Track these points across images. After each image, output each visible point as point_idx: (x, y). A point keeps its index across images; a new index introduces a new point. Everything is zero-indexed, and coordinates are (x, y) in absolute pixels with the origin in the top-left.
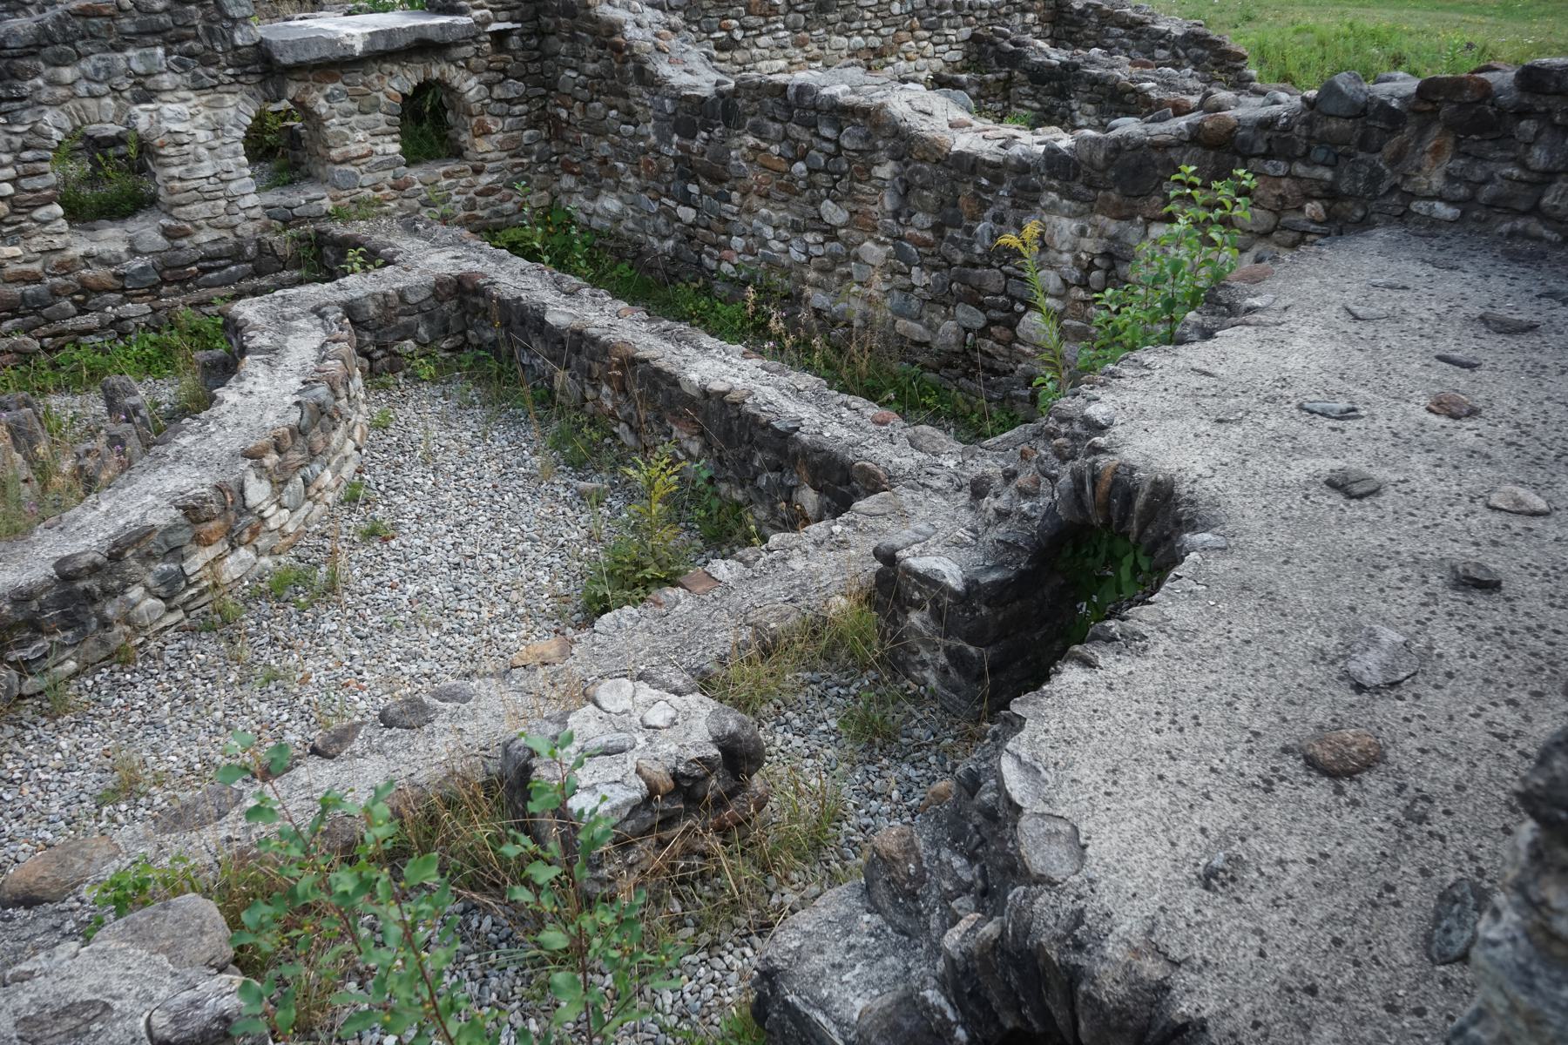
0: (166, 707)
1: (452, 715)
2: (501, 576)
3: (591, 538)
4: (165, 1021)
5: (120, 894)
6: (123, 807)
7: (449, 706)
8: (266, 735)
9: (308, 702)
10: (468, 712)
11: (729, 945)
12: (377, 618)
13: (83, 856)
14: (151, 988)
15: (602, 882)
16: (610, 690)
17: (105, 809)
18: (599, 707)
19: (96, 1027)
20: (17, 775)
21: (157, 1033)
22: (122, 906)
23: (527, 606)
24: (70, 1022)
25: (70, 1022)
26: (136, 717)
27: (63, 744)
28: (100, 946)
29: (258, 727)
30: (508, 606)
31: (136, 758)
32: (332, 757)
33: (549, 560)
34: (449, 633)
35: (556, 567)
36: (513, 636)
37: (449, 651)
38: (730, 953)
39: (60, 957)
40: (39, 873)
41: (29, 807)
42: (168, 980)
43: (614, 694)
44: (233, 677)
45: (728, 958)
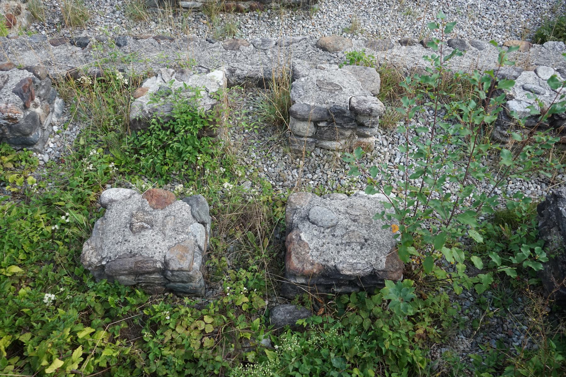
0: (373, 9)
1: (473, 52)
2: (507, 11)
3: (552, 11)
4: (355, 101)
5: (353, 58)
6: (349, 36)
7: (474, 49)
8: (399, 33)
9: (417, 28)
10: (480, 54)
11: (533, 181)
12: (453, 8)
13: (343, 42)
14: (354, 90)
15: (502, 135)
16: (544, 70)
17: (344, 34)
18: (537, 74)
19: (337, 93)
20: (324, 11)
21: (352, 103)
22: (352, 62)
23: (511, 27)
24: (330, 87)
25: (330, 87)
26: (363, 8)
27: (339, 7)
28: (344, 70)
29: (398, 29)
30: (503, 24)
31: (358, 22)
32: (426, 48)
33: (529, 12)
34: (476, 24)
35: (530, 16)
36: (500, 36)
37: (473, 31)
38: (532, 184)
39: (333, 68)
40: (330, 42)
41: (324, 23)
42: (360, 90)
43: (545, 72)
44: (397, 7)
45: (530, 185)
